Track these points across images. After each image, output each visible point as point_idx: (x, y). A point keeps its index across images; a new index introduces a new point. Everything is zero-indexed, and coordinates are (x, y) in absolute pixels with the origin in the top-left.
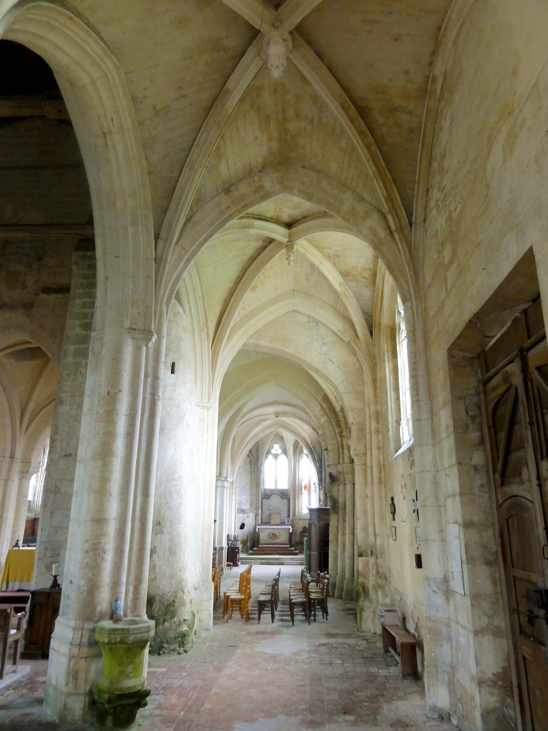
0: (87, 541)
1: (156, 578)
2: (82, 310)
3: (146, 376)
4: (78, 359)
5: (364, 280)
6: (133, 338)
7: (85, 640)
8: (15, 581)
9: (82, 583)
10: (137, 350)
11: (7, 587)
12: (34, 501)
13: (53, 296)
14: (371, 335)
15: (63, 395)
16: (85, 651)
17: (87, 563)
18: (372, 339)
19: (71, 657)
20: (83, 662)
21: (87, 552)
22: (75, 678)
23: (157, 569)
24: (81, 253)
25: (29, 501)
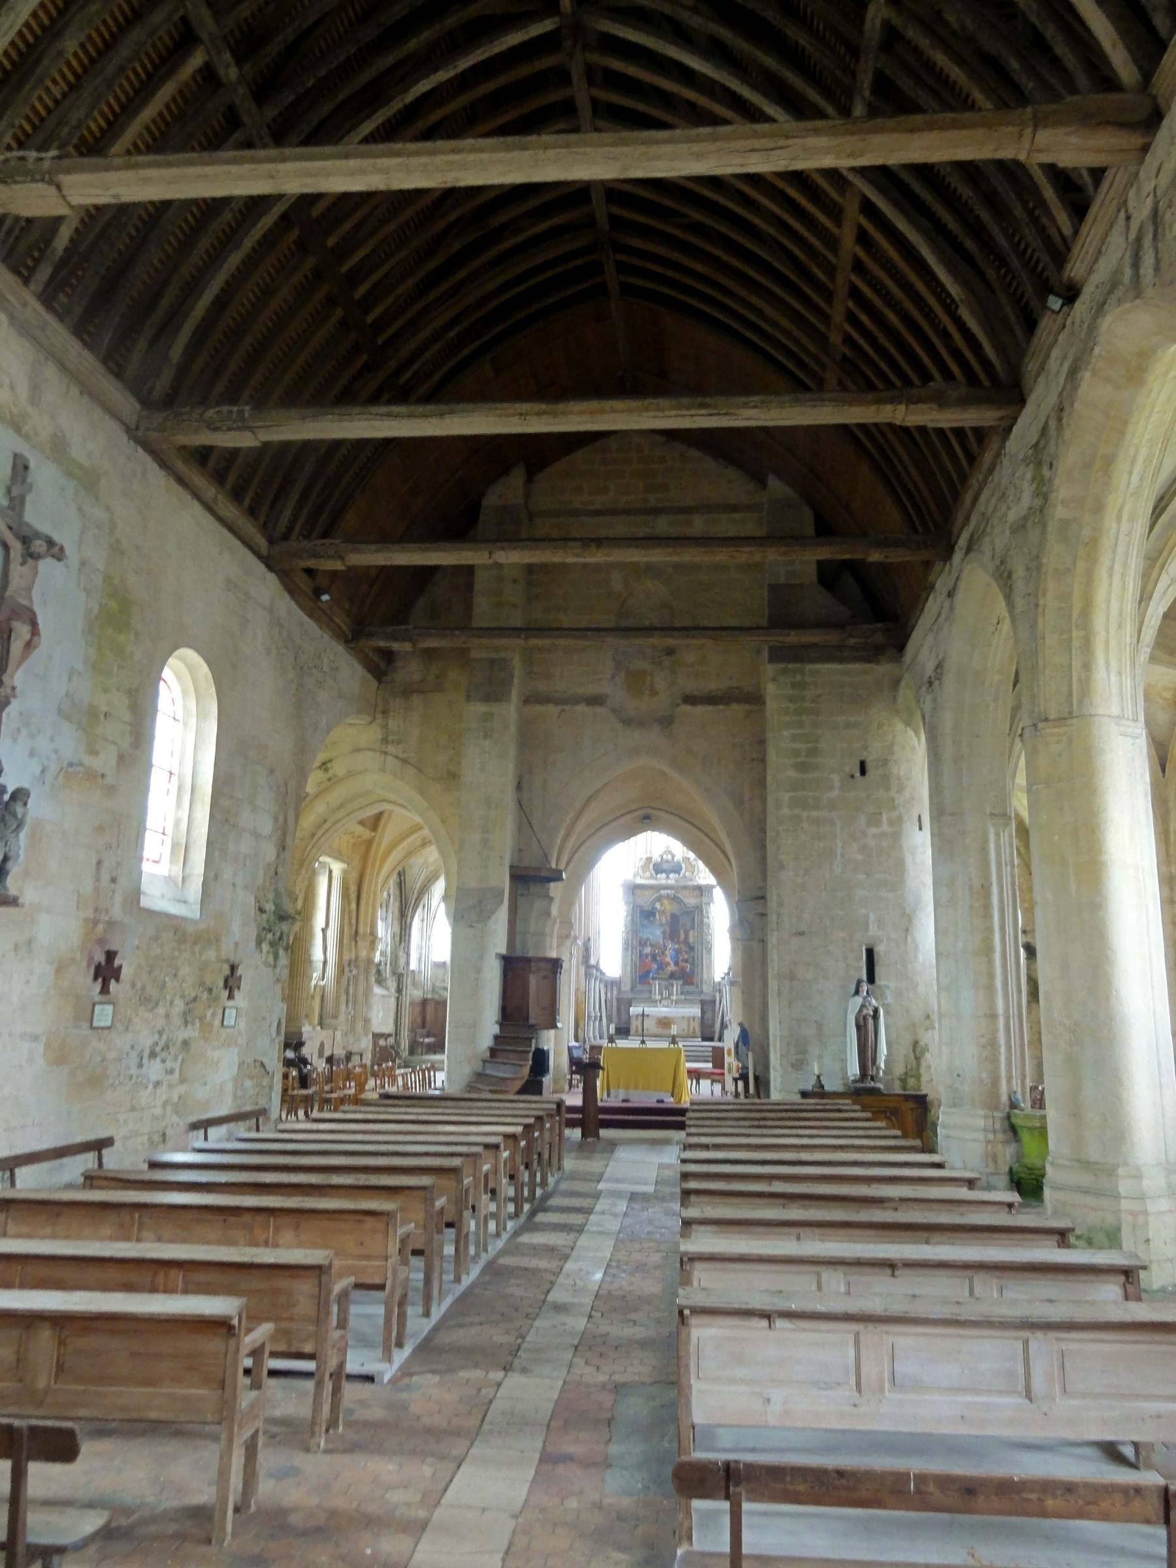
0: (983, 1036)
1: (932, 1080)
2: (794, 745)
3: (1006, 865)
4: (797, 811)
5: (1161, 701)
6: (994, 825)
7: (998, 1126)
8: (618, 1087)
9: (984, 1075)
10: (997, 835)
11: (609, 1095)
12: (420, 972)
13: (700, 709)
14: (1163, 770)
15: (782, 857)
16: (1000, 1137)
17: (986, 1057)
18: (1164, 776)
19: (988, 1142)
20: (1000, 1146)
21: (984, 1047)
22: (995, 1161)
23: (932, 1069)
24: (781, 666)
25: (413, 971)
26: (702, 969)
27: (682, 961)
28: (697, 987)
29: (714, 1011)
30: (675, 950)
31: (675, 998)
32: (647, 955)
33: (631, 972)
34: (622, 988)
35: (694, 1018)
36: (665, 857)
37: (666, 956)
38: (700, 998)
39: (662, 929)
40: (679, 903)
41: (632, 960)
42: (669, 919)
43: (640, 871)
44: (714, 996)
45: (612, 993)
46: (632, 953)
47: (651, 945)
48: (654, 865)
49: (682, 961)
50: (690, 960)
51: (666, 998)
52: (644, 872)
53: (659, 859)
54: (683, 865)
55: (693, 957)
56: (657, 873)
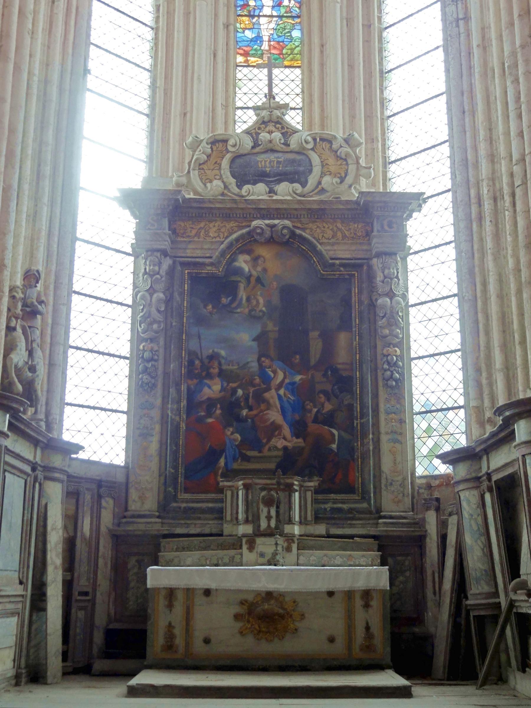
26: (377, 442)
27: (316, 420)
28: (365, 497)
29: (420, 570)
30: (293, 387)
31: (297, 530)
32: (211, 403)
33: (161, 455)
34: (134, 506)
35: (367, 594)
36: (264, 136)
37: (269, 406)
38: (373, 531)
39: (257, 330)
40: (308, 258)
41: (164, 416)
42: (276, 300)
43: (195, 175)
44: (421, 524)
45: (97, 518)
46: (165, 398)
47: (222, 374)
48: (233, 161)
49: (316, 420)
50: (340, 417)
51: (269, 534)
52: (206, 180)
53: (248, 142)
54: (315, 159)
55: (350, 408)
56: (241, 181)
